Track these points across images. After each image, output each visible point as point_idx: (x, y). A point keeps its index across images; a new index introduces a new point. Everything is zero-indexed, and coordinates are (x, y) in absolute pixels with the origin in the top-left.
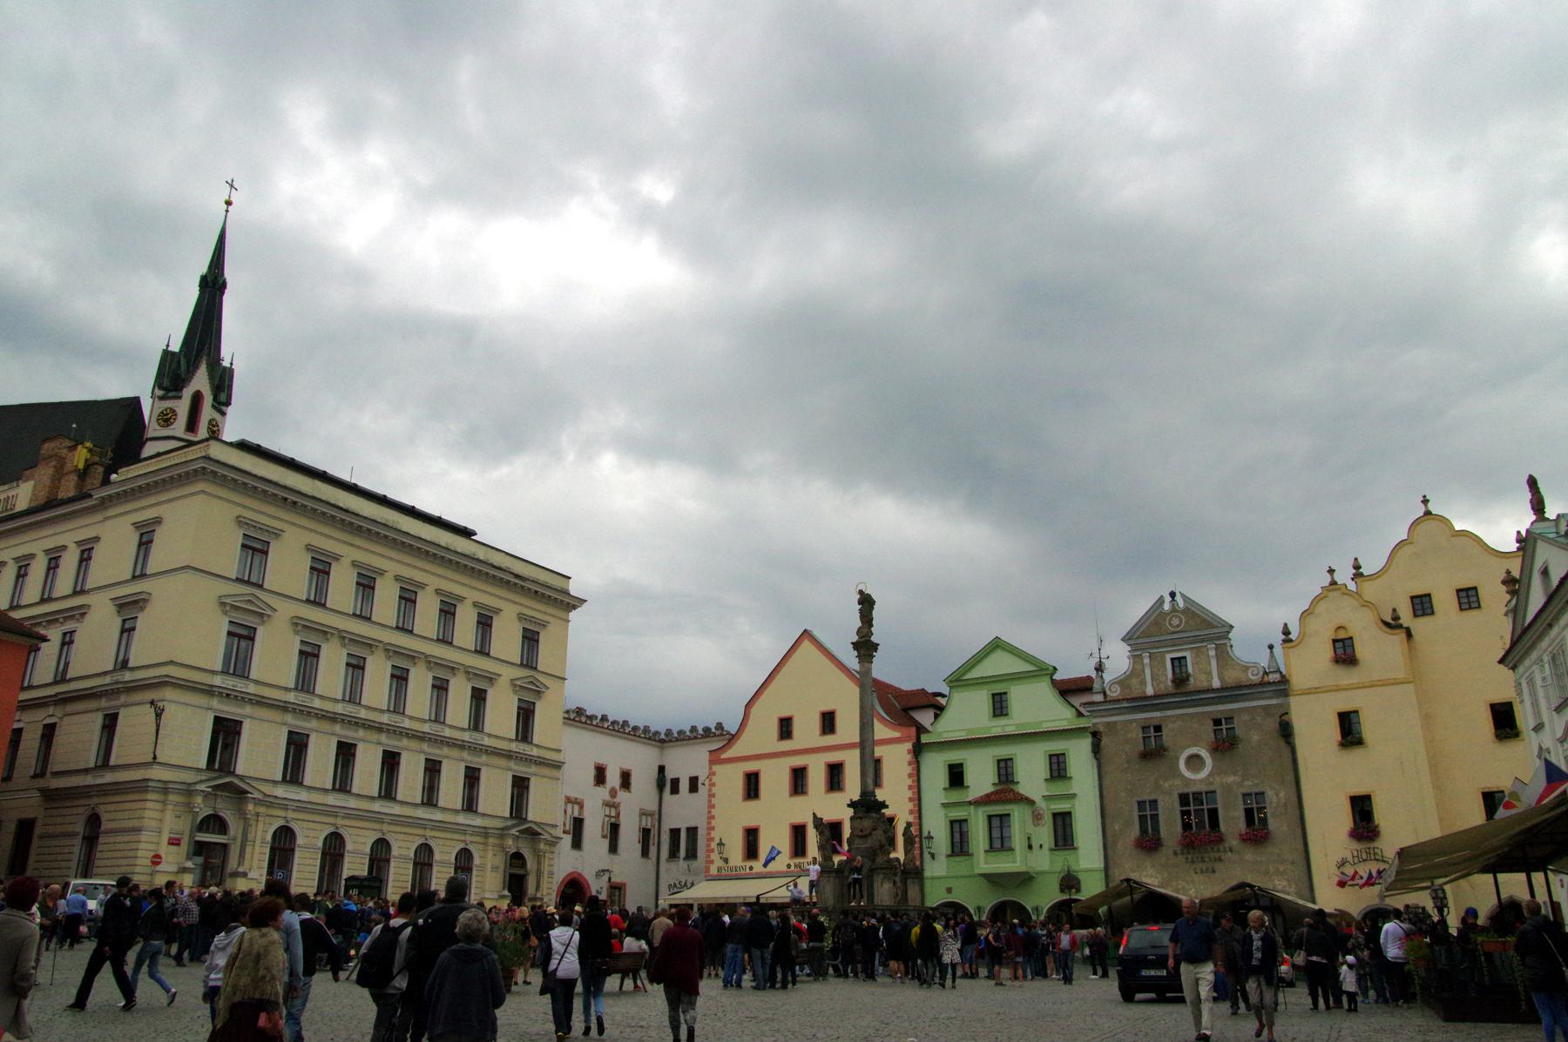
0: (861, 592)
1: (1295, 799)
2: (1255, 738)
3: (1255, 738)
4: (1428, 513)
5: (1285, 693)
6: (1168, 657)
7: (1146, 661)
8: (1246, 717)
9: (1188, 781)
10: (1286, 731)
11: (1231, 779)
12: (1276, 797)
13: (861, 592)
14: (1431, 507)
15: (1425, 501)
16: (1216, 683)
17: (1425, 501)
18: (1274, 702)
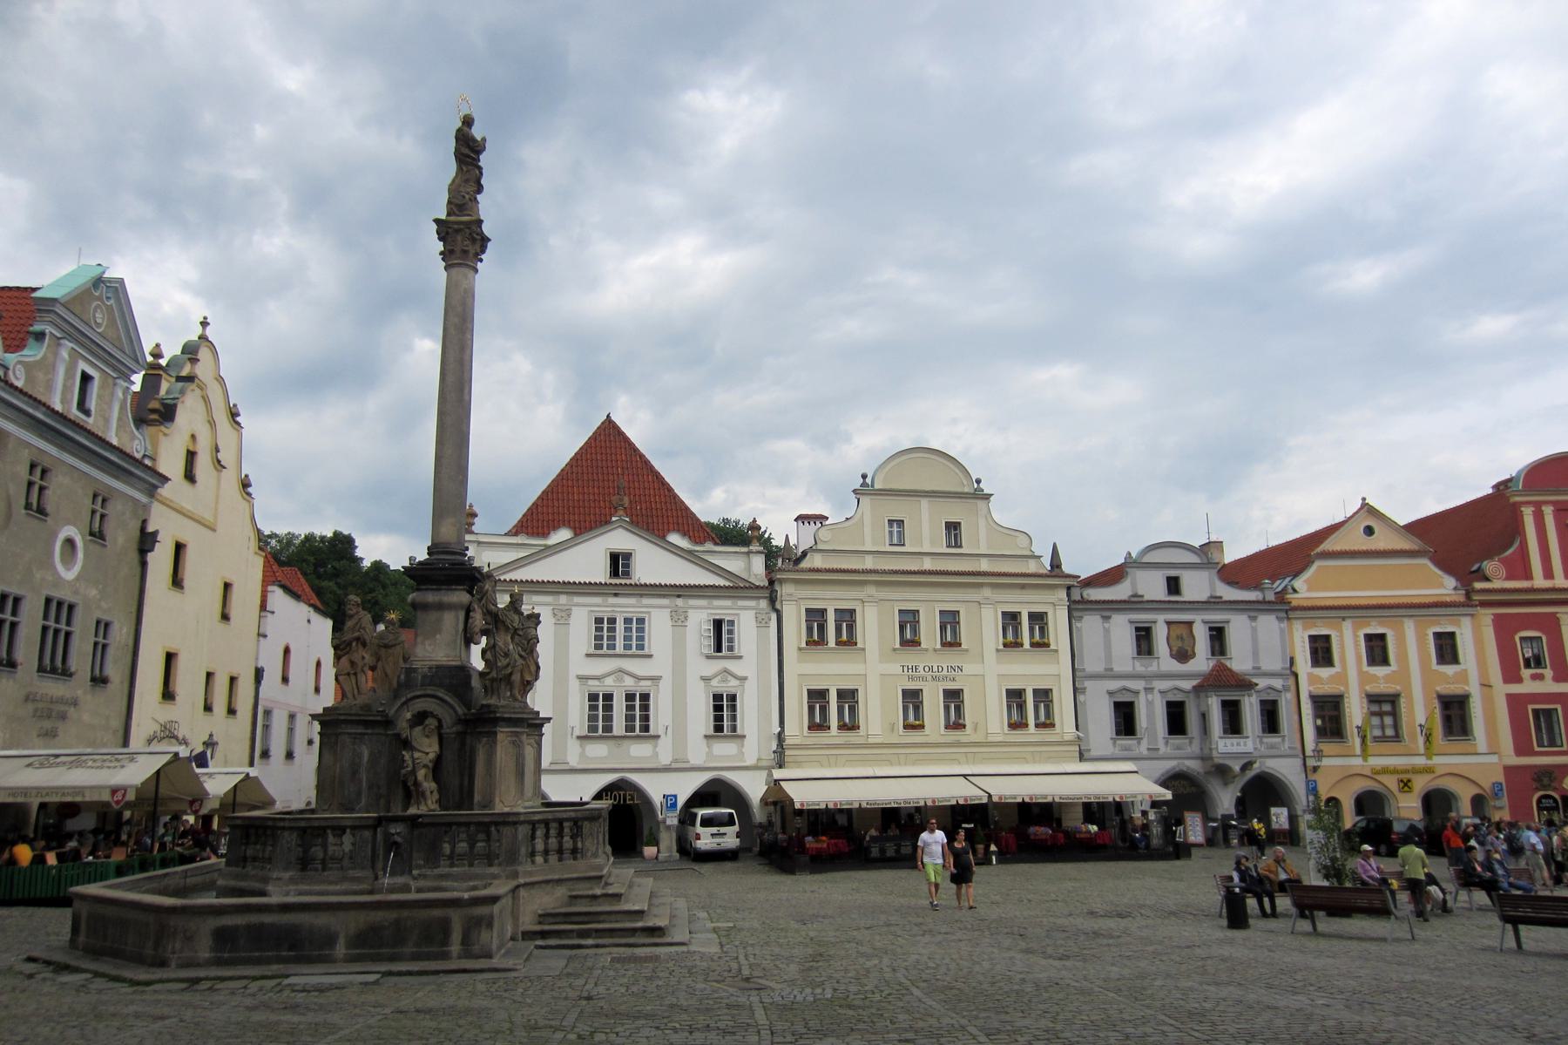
0: (468, 121)
1: (131, 643)
2: (121, 540)
3: (121, 540)
4: (203, 338)
5: (151, 491)
6: (83, 366)
7: (65, 354)
8: (119, 507)
9: (59, 581)
10: (146, 541)
11: (93, 592)
12: (120, 634)
13: (468, 121)
14: (209, 332)
15: (204, 324)
16: (115, 442)
17: (204, 324)
18: (144, 499)
